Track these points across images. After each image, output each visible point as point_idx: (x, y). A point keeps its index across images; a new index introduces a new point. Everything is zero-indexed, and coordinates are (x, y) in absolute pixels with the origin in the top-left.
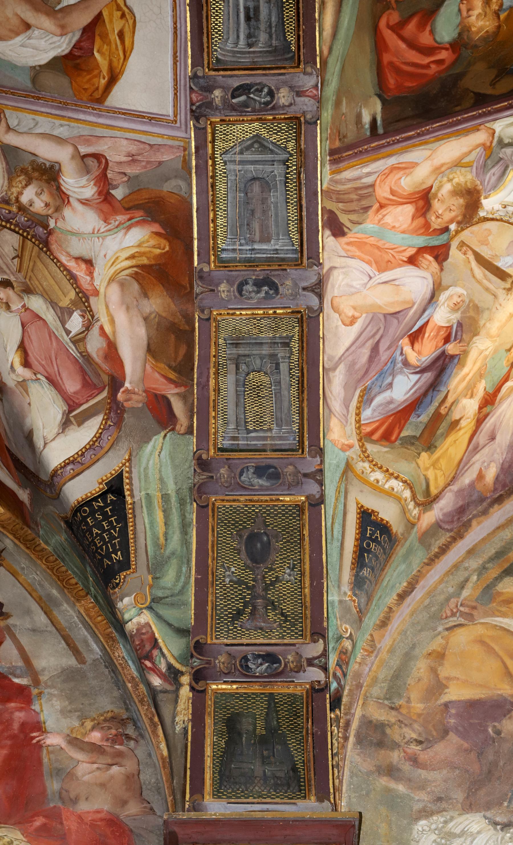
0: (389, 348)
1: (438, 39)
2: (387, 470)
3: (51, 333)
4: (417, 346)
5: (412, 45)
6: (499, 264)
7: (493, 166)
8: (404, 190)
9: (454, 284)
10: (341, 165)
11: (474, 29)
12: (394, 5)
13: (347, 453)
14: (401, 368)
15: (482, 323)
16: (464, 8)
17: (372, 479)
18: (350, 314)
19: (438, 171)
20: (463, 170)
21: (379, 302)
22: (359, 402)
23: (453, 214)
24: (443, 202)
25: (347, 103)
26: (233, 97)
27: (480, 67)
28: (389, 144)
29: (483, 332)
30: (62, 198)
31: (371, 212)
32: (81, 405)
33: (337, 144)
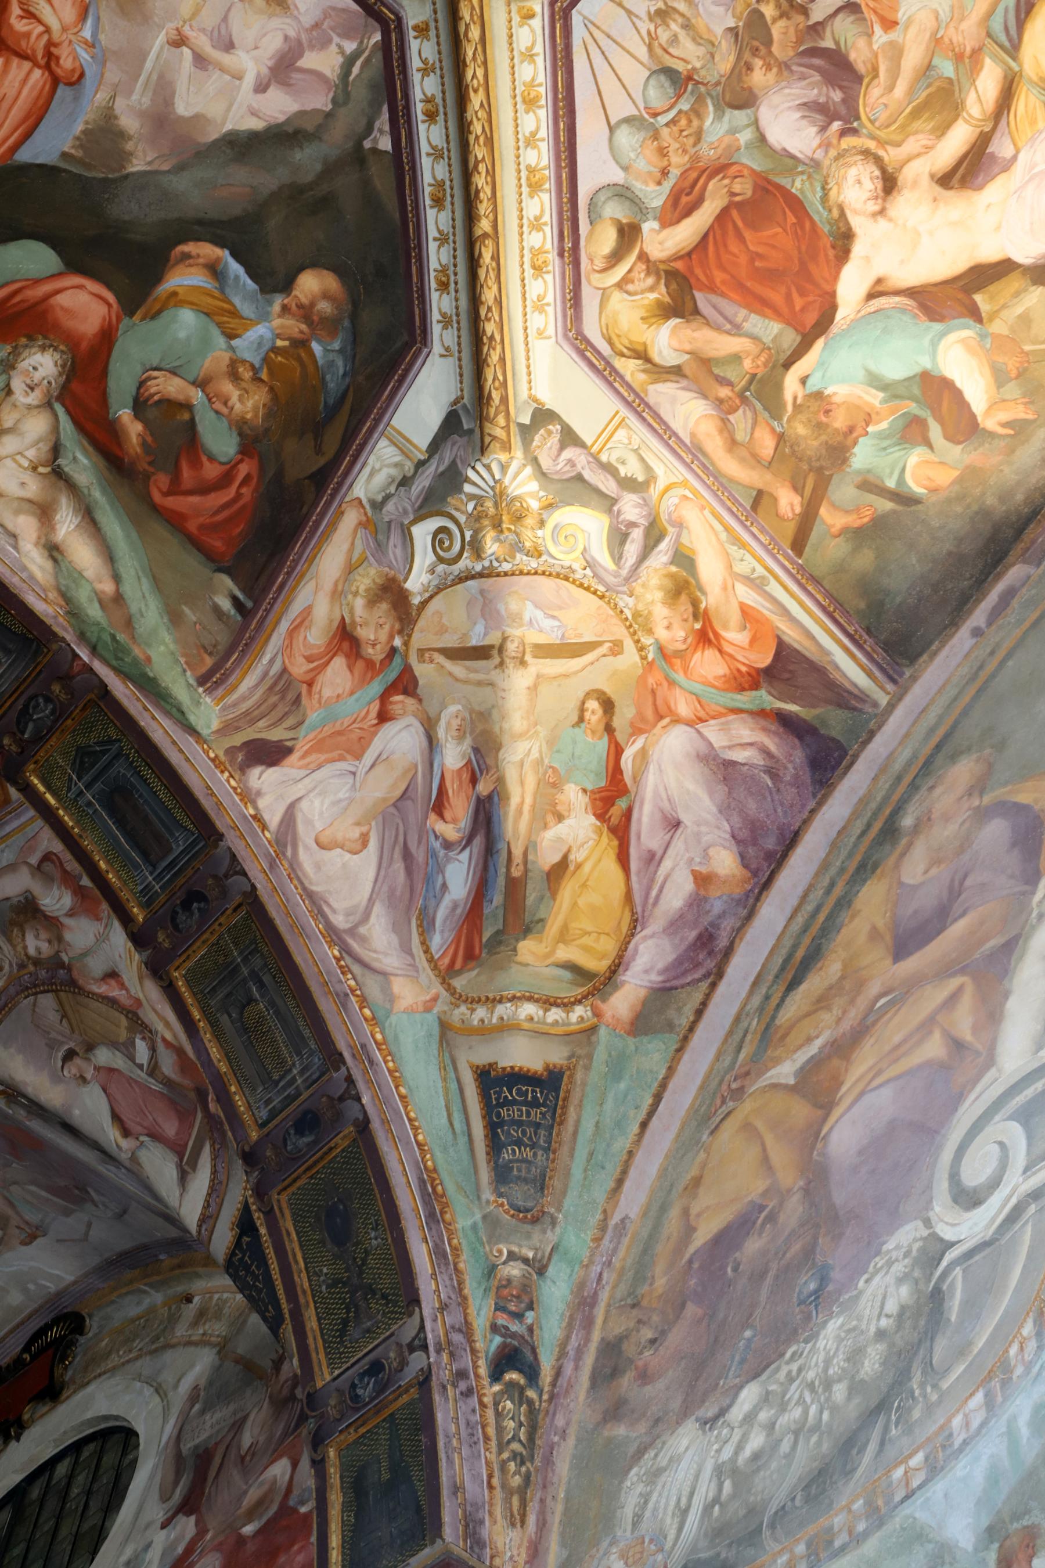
0: (419, 842)
1: (223, 460)
2: (487, 998)
3: (130, 1081)
4: (448, 815)
5: (205, 489)
6: (474, 642)
7: (388, 538)
8: (319, 647)
9: (444, 706)
10: (232, 679)
11: (249, 416)
12: (151, 469)
13: (435, 1010)
14: (446, 855)
15: (497, 729)
16: (218, 406)
17: (476, 1023)
18: (357, 835)
19: (337, 594)
20: (360, 570)
21: (378, 794)
22: (421, 934)
23: (387, 627)
24: (365, 624)
25: (191, 609)
26: (23, 733)
27: (291, 445)
28: (268, 611)
29: (506, 739)
30: (53, 925)
31: (304, 700)
32: (187, 1144)
33: (209, 662)
